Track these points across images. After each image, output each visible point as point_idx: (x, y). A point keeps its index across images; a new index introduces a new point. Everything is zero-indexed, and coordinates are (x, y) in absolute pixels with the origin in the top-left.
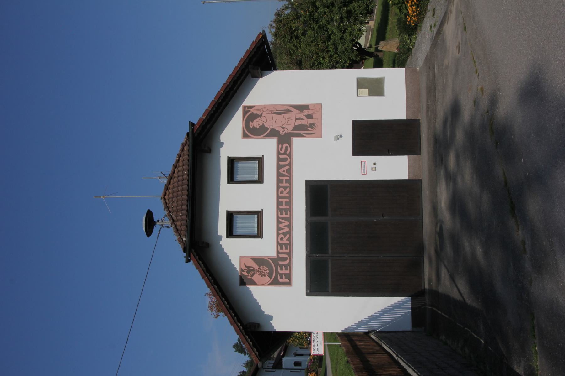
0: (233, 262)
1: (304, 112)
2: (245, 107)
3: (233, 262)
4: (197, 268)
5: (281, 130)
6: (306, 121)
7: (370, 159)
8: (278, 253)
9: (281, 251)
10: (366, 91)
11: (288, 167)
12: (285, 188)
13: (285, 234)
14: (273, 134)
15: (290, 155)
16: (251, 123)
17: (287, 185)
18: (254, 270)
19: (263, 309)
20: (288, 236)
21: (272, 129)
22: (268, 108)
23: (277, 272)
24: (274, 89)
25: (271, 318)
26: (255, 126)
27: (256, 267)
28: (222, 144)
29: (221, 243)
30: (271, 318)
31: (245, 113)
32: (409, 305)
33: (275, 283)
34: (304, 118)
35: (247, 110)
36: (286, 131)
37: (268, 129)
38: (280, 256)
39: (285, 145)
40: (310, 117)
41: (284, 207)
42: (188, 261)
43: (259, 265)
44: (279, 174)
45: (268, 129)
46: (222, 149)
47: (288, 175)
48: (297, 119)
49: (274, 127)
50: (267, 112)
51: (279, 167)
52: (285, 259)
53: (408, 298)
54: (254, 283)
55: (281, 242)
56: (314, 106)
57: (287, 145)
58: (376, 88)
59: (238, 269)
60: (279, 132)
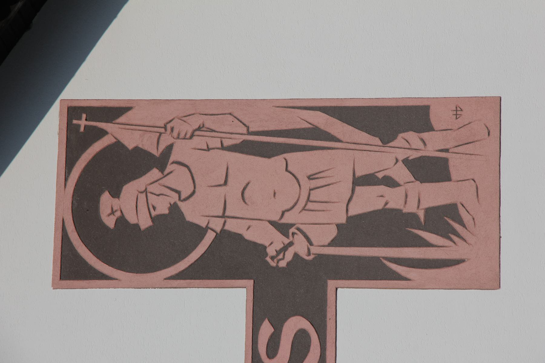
1: (399, 141)
2: (73, 112)
14: (229, 259)
16: (106, 199)
22: (200, 119)
26: (132, 219)
31: (75, 142)
34: (402, 174)
35: (86, 125)
36: (300, 247)
39: (295, 324)
40: (430, 169)
45: (199, 232)
48: (360, 181)
49: (232, 226)
50: (197, 141)
56: (457, 112)
57: (304, 324)
60: (261, 249)
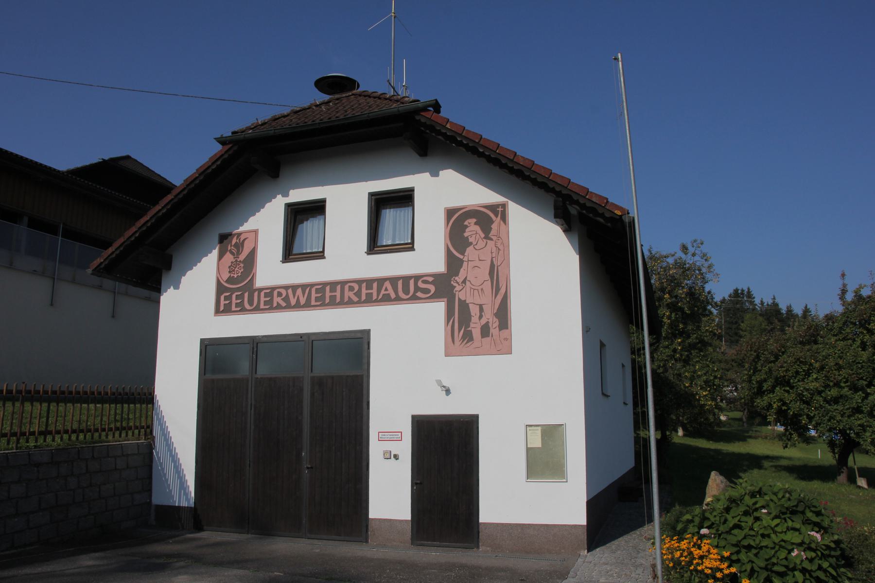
0: (251, 219)
1: (495, 319)
2: (504, 206)
3: (251, 220)
4: (210, 159)
5: (460, 278)
6: (478, 323)
7: (405, 448)
8: (260, 290)
9: (262, 294)
10: (536, 442)
11: (393, 296)
12: (358, 294)
13: (286, 299)
14: (454, 263)
15: (414, 298)
16: (475, 220)
17: (364, 298)
18: (239, 253)
19: (189, 273)
20: (284, 304)
21: (462, 261)
22: (503, 249)
23: (233, 291)
24: (543, 261)
25: (177, 287)
26: (467, 230)
27: (242, 257)
28: (435, 174)
29: (279, 197)
30: (177, 287)
31: (493, 208)
32: (184, 504)
33: (220, 289)
34: (484, 321)
35: (500, 211)
36: (458, 288)
37: (463, 254)
38: (256, 294)
39: (432, 288)
40: (485, 331)
41: (328, 294)
42: (222, 141)
43: (244, 262)
44: (381, 281)
45: (463, 254)
46: (427, 175)
47: (380, 297)
48: (481, 306)
49: (465, 264)
50: (494, 249)
51: (393, 280)
52: (251, 302)
53: (192, 504)
54: (221, 256)
55: (275, 293)
56: (506, 339)
57: (432, 292)
58: (543, 462)
59: (241, 229)
60: (457, 274)
